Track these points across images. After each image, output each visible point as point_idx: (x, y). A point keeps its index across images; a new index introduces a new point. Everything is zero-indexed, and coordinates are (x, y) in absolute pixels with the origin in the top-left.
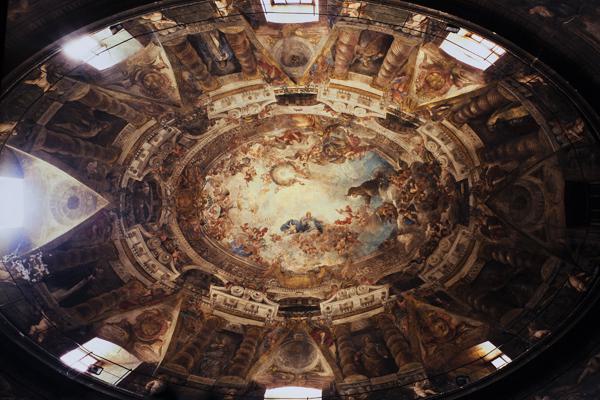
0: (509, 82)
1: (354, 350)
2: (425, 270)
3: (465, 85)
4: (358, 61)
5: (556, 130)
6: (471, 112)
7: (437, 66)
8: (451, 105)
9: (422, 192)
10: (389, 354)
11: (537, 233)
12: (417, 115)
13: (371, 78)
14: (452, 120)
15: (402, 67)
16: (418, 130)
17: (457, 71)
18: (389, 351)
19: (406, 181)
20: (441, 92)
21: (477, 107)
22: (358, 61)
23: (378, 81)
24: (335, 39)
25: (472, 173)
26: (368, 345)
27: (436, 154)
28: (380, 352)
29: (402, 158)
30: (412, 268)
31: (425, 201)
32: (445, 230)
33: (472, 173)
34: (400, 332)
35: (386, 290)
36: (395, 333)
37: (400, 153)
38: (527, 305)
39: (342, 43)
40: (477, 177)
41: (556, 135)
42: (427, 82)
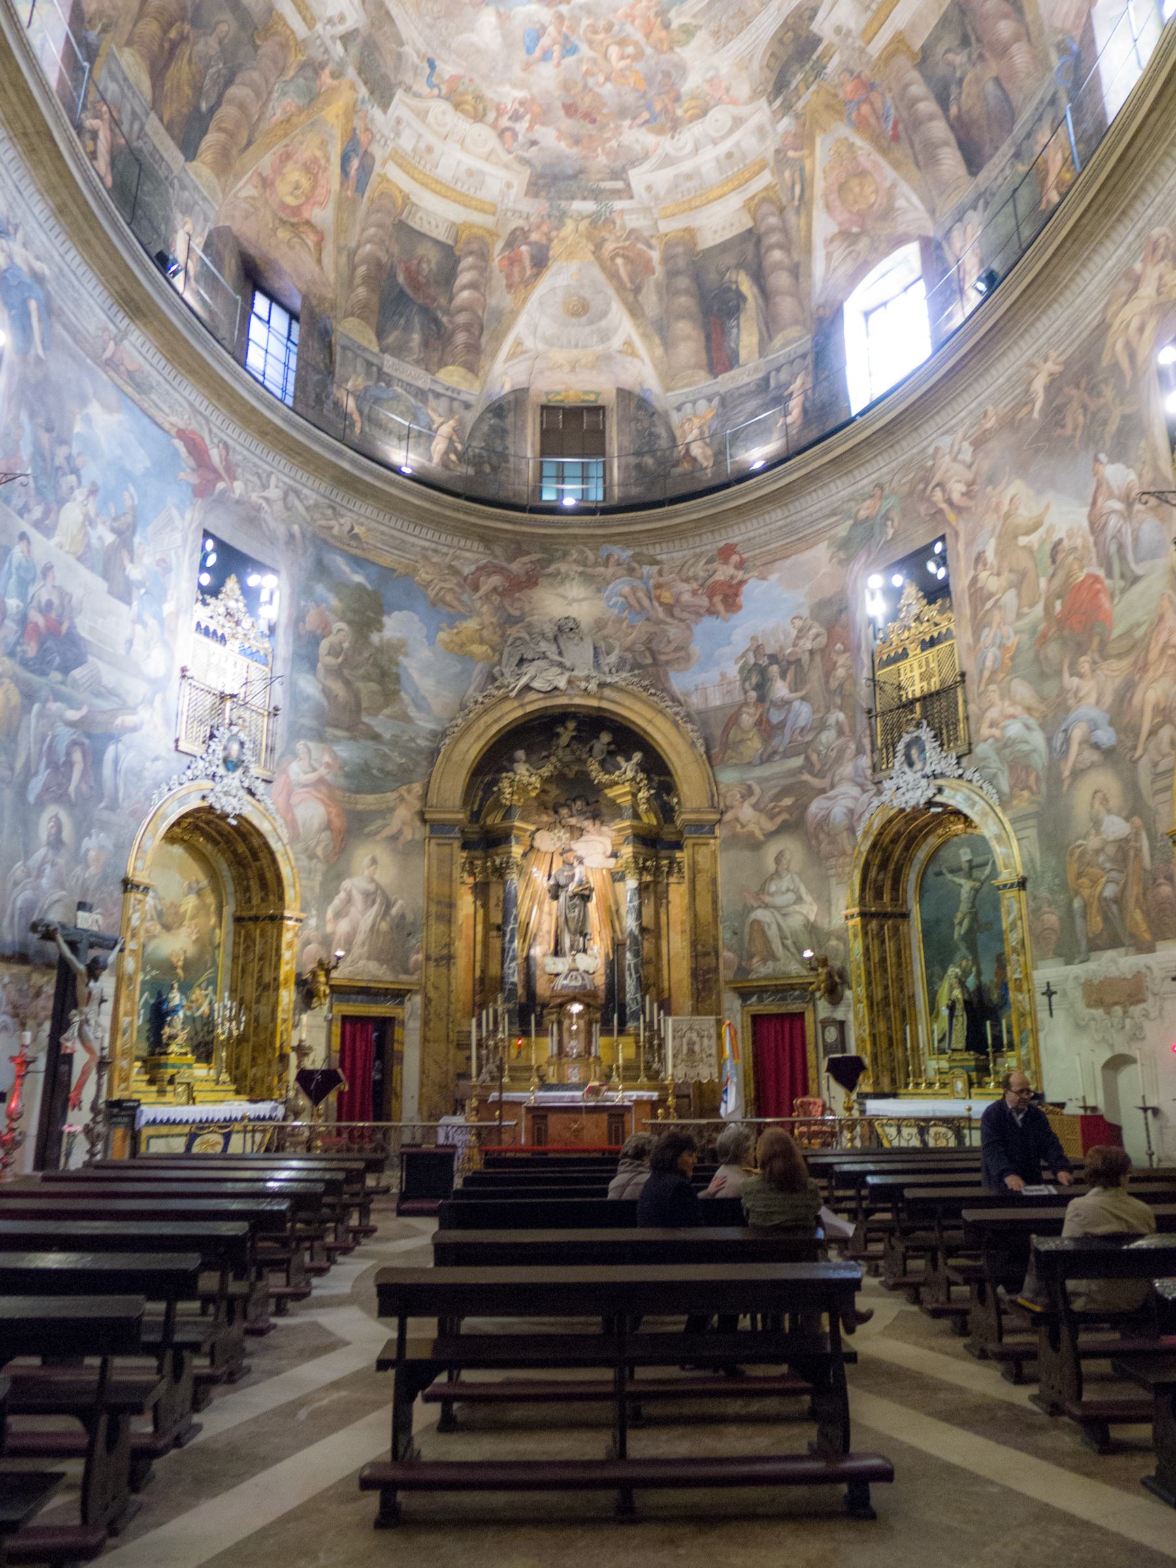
0: (804, 356)
1: (190, 15)
2: (415, 102)
3: (829, 256)
4: (965, 42)
5: (702, 405)
6: (771, 247)
7: (888, 212)
8: (798, 211)
9: (608, 79)
10: (212, 110)
11: (518, 343)
12: (797, 116)
13: (917, 45)
14: (767, 197)
15: (912, 146)
16: (763, 102)
17: (863, 244)
18: (218, 103)
19: (638, 36)
20: (833, 197)
21: (778, 266)
22: (965, 42)
23: (903, 61)
24: (1034, 33)
25: (647, 210)
26: (213, 41)
27: (697, 129)
28: (207, 81)
29: (701, 35)
30: (415, 68)
31: (585, 86)
32: (515, 135)
33: (647, 210)
34: (265, 105)
35: (349, 25)
36: (258, 94)
37: (716, 34)
38: (387, 357)
39: (1017, 38)
40: (634, 222)
41: (694, 402)
42: (862, 174)
